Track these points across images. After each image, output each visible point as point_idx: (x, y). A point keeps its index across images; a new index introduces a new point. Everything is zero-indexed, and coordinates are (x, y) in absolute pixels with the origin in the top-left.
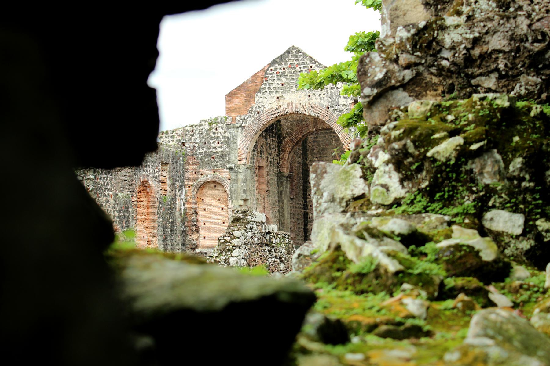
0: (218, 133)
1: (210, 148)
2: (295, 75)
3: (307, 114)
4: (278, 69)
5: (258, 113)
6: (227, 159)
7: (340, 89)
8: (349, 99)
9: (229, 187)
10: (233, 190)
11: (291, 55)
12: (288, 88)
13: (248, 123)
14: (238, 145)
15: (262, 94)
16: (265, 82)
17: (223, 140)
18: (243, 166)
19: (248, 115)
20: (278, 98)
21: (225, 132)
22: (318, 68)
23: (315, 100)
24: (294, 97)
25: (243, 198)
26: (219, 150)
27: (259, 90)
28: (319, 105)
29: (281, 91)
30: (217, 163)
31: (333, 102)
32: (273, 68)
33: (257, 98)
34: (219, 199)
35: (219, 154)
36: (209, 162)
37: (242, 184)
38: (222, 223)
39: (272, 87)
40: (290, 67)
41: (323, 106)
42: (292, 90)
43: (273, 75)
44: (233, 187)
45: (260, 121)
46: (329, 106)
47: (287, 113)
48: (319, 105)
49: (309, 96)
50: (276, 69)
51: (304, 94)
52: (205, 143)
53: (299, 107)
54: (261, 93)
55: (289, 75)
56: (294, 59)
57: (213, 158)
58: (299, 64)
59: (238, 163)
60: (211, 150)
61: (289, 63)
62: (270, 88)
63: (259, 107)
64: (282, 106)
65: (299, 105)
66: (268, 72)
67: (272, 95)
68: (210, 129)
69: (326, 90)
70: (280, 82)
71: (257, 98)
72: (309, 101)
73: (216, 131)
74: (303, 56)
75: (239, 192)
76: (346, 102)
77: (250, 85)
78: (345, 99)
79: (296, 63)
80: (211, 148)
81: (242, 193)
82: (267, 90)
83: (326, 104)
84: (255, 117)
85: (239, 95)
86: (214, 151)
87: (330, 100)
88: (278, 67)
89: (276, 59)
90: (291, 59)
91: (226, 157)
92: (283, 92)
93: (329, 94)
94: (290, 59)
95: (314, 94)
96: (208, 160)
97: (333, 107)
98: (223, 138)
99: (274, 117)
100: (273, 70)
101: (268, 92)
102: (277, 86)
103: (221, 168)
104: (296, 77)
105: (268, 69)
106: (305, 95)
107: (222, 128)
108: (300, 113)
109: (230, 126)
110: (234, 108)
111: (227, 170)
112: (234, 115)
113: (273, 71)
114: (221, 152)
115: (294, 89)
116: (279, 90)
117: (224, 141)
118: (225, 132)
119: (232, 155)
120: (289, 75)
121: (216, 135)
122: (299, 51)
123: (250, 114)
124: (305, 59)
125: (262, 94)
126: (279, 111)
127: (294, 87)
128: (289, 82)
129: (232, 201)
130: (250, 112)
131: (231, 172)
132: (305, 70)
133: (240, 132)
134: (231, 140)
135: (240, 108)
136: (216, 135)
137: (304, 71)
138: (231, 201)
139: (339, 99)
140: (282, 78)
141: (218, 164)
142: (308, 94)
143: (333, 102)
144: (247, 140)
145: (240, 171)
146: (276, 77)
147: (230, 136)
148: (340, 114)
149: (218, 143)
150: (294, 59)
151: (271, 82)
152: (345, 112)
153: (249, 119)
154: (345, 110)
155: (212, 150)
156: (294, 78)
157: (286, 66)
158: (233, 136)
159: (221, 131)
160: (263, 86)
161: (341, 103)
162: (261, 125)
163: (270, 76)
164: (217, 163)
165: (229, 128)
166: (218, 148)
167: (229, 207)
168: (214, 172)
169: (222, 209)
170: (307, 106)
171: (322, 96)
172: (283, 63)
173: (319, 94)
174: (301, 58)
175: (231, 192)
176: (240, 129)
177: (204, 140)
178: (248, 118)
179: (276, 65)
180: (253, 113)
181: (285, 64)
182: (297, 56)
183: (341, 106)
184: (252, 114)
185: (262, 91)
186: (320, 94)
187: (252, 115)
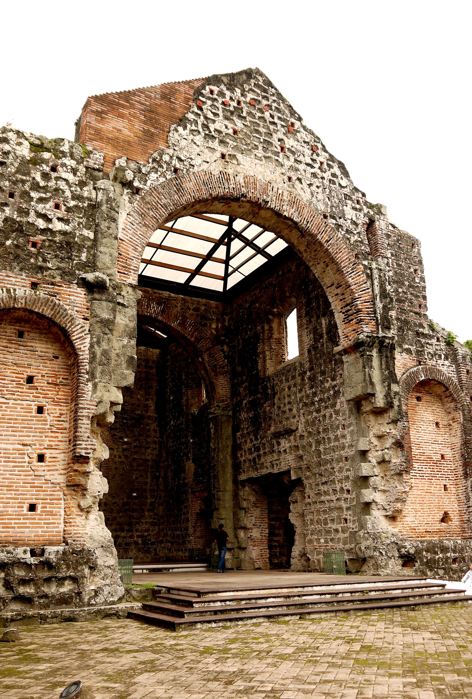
0: (57, 179)
1: (27, 214)
2: (261, 124)
3: (286, 214)
4: (228, 98)
5: (176, 170)
6: (84, 257)
7: (345, 189)
8: (362, 216)
9: (88, 340)
10: (98, 351)
11: (255, 84)
12: (246, 145)
13: (149, 183)
14: (120, 230)
15: (187, 131)
16: (196, 110)
17: (72, 203)
18: (130, 290)
19: (150, 165)
20: (223, 156)
21: (82, 184)
22: (305, 132)
23: (301, 193)
24: (260, 169)
25: (125, 384)
26: (58, 226)
27: (182, 121)
28: (310, 204)
29: (231, 142)
30: (45, 260)
31: (334, 210)
32: (215, 89)
33: (176, 135)
34: (30, 380)
35: (57, 239)
36: (19, 252)
37: (125, 341)
38: (35, 456)
39: (212, 127)
40: (251, 104)
41: (317, 209)
42: (256, 152)
43: (215, 103)
44: (98, 343)
45: (180, 189)
46: (328, 214)
47: (243, 195)
48: (310, 204)
49: (290, 179)
50: (221, 94)
51: (279, 170)
52: (12, 195)
53: (270, 193)
54: (185, 128)
55: (248, 118)
56: (259, 92)
57: (34, 245)
58: (270, 106)
59: (118, 278)
60: (30, 220)
61: (250, 96)
62: (208, 128)
63: (180, 160)
64: (232, 178)
65: (270, 188)
66: (203, 91)
67: (210, 144)
68: (35, 162)
69: (321, 180)
70: (230, 125)
71: (174, 137)
72: (290, 189)
73: (54, 175)
74: (276, 95)
75: (113, 362)
76: (357, 219)
77: (158, 102)
78: (355, 212)
79: (265, 102)
80: (32, 213)
81: (124, 366)
82: (201, 130)
83: (321, 207)
84: (168, 177)
85: (126, 112)
86: (41, 224)
87: (329, 203)
88: (228, 93)
89: (222, 75)
90: (253, 91)
91: (80, 251)
92: (235, 148)
93: (327, 190)
94: (251, 90)
95: (299, 180)
96: (17, 246)
97: (334, 218)
98: (73, 198)
99: (214, 194)
100: (216, 92)
101: (203, 134)
102: (223, 129)
103: (58, 279)
104: (265, 130)
105: (204, 88)
106: (283, 174)
107: (74, 171)
108: (273, 206)
109: (96, 173)
110: (110, 136)
111: (81, 292)
112: (111, 152)
113: (215, 96)
114: (64, 233)
115: (260, 152)
116: (228, 140)
117: (76, 206)
118: (82, 184)
119: (102, 249)
120: (248, 118)
121: (52, 184)
122: (270, 84)
123: (155, 165)
124: (281, 104)
125: (187, 131)
126: (226, 184)
127: (260, 148)
128: (248, 133)
129: (95, 386)
130: (154, 160)
131: (97, 296)
132: (283, 126)
133: (127, 198)
134: (104, 208)
135: (129, 143)
136: (52, 184)
137: (279, 126)
138: (90, 384)
139: (345, 207)
140: (234, 118)
141: (50, 265)
142: (288, 174)
143: (334, 210)
144: (145, 225)
145: (121, 301)
146: (220, 109)
147: (101, 196)
148: (349, 237)
149: (57, 206)
150: (259, 92)
151: (210, 115)
152: (356, 237)
153: (153, 176)
154: (355, 232)
155: (32, 218)
156: (262, 130)
157: (244, 100)
158: (109, 200)
159: (70, 177)
160: (191, 116)
161: (348, 216)
162: (183, 201)
163: (209, 102)
164: (45, 260)
165: (95, 179)
166: (55, 220)
167: (83, 403)
168: (34, 286)
169: (40, 410)
170: (285, 198)
171: (314, 188)
172: (238, 91)
173: (309, 182)
174: (275, 98)
175: (93, 356)
176: (126, 191)
177: (7, 183)
178: (149, 173)
179: (223, 87)
180: (165, 166)
181: (242, 95)
182: (265, 91)
183: (349, 221)
184: (161, 167)
185: (189, 126)
186: (310, 185)
187: (160, 169)
